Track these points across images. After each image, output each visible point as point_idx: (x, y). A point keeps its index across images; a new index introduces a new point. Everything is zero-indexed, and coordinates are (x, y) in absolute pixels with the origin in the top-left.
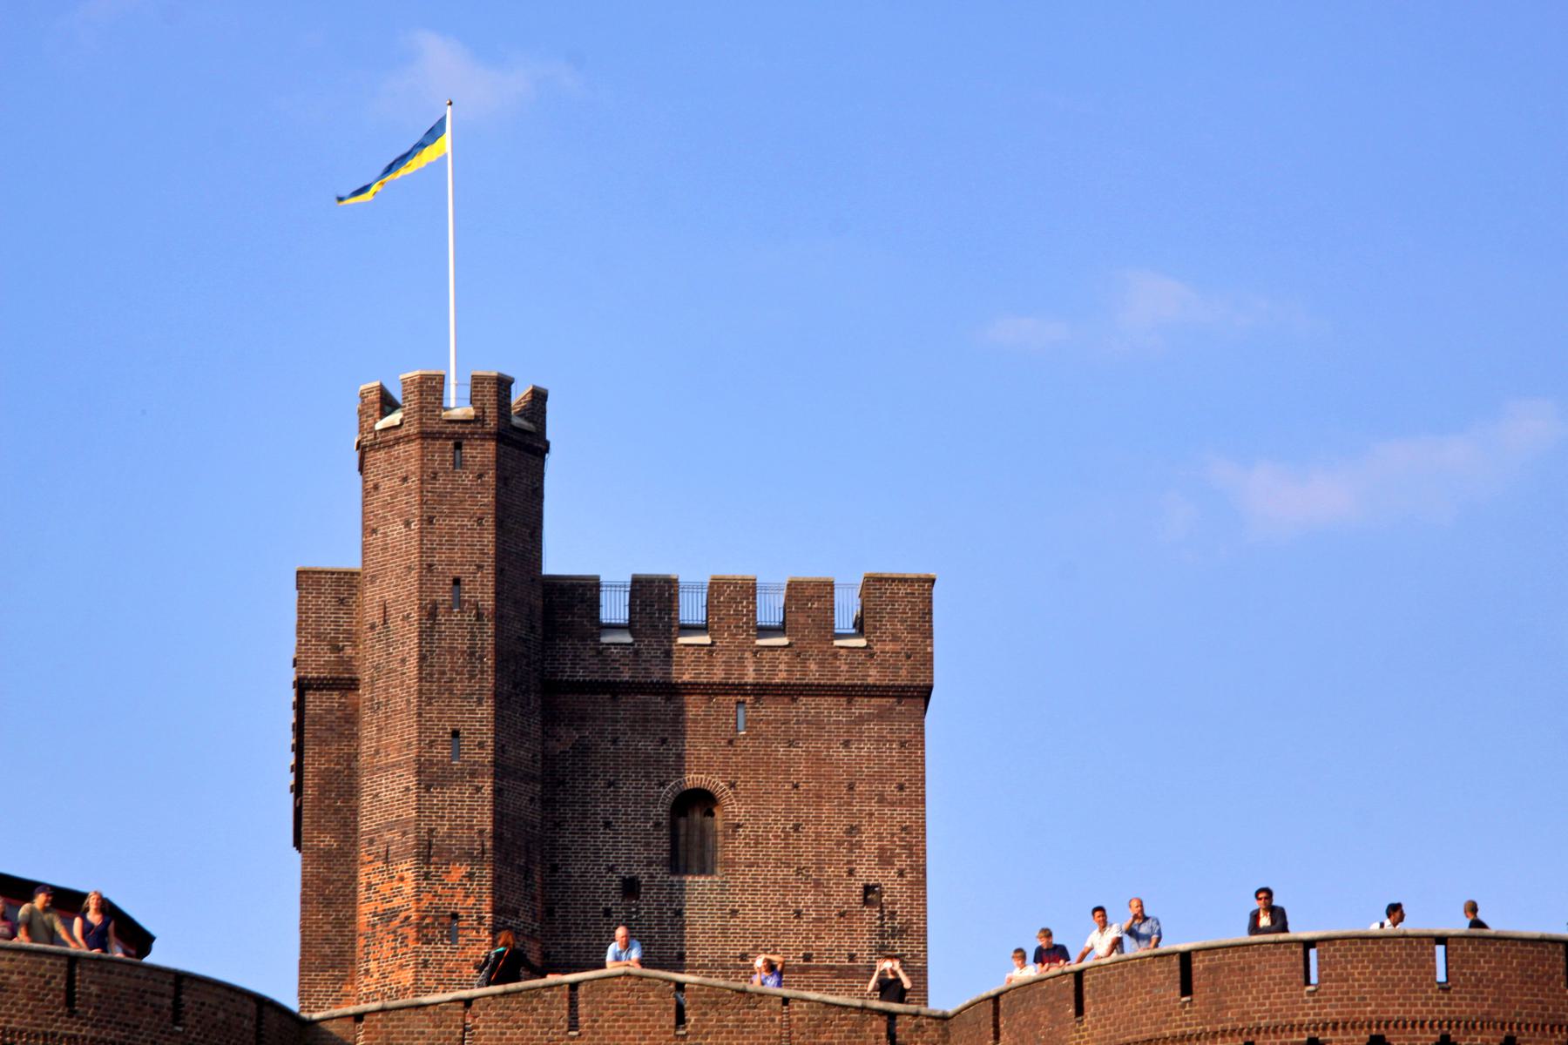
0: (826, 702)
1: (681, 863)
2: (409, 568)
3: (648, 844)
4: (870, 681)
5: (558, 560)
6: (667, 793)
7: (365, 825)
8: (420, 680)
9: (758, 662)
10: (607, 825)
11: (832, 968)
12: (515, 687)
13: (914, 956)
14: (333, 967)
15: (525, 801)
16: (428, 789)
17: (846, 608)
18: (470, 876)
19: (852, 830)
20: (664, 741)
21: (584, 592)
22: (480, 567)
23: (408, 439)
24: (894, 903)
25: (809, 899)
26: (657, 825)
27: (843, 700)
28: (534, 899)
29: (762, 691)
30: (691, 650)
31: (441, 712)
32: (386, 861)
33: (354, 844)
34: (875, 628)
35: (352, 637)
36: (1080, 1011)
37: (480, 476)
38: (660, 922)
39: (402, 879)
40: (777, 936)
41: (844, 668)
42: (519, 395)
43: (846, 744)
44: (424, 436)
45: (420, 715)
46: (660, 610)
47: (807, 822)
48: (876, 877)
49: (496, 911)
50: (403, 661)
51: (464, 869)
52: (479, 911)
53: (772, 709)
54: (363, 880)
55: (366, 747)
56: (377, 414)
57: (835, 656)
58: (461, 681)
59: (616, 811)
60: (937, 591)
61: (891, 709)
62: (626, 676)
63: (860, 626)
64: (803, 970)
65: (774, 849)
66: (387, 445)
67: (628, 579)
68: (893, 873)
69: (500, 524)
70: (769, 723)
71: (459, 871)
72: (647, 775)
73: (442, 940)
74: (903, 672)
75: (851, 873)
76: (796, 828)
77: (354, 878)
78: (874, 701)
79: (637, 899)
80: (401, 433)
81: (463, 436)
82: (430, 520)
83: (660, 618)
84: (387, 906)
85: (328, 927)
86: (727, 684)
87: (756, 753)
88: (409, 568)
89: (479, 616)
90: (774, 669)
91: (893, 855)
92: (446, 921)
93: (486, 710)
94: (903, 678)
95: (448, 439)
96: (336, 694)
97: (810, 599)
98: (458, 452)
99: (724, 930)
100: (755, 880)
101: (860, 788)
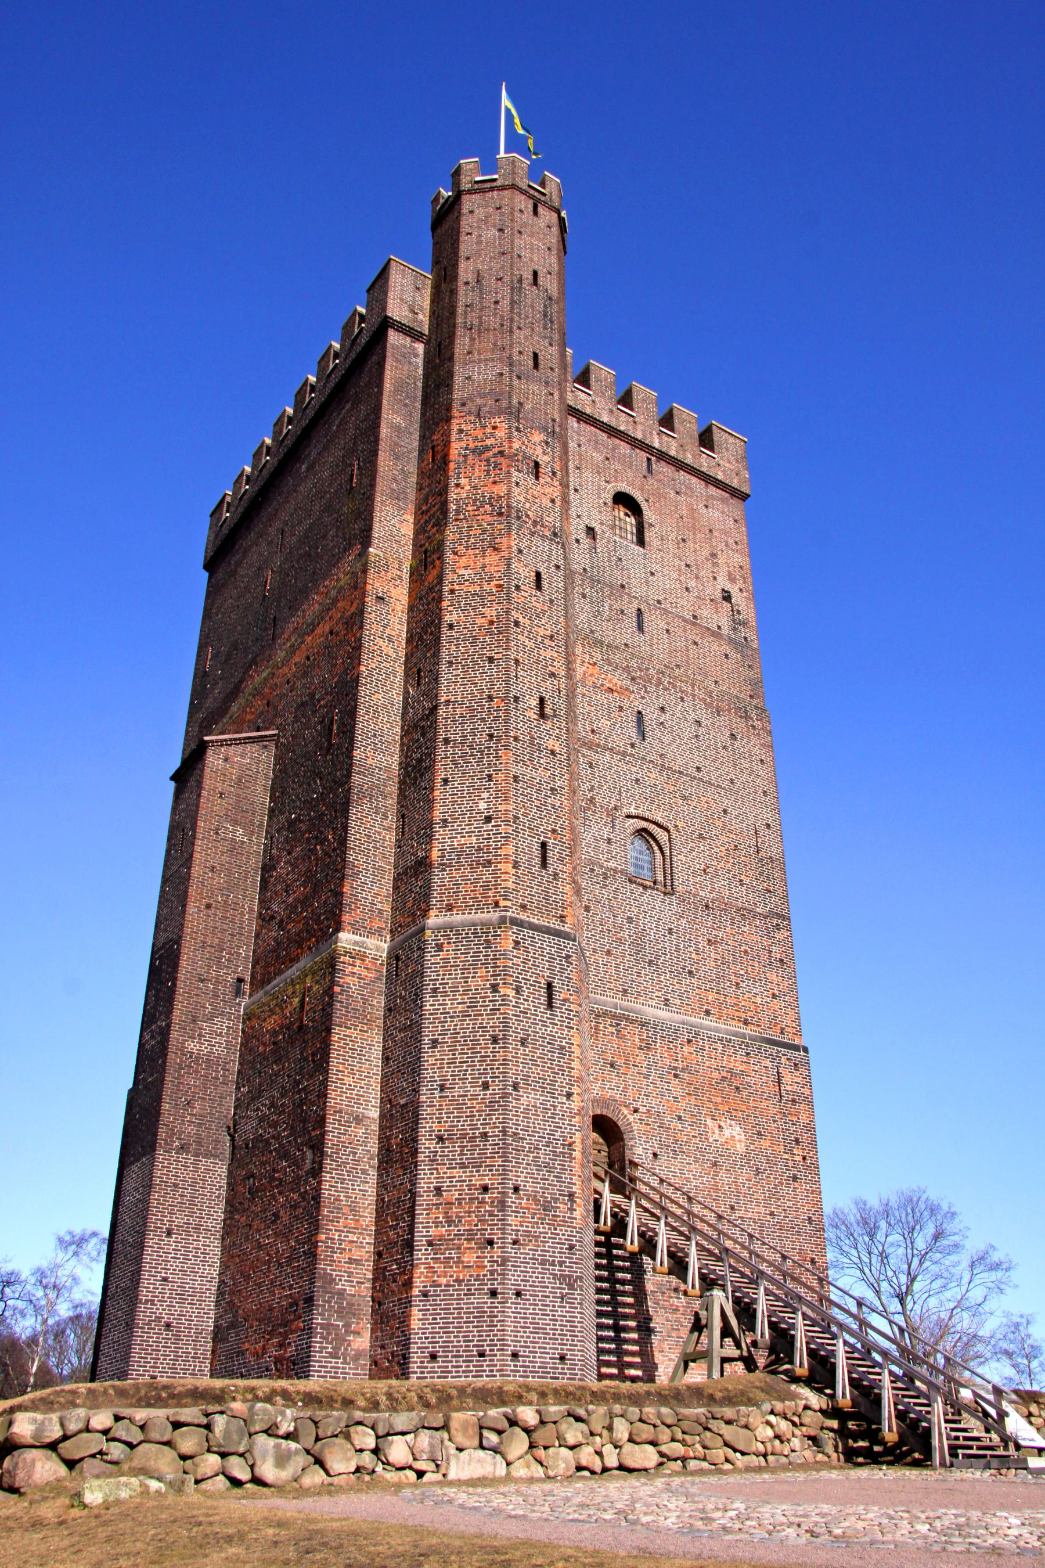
0: (694, 480)
6: (611, 489)
11: (709, 629)
19: (714, 555)
23: (503, 188)
29: (663, 456)
32: (479, 416)
38: (609, 561)
48: (728, 587)
65: (671, 546)
66: (483, 191)
72: (598, 473)
75: (715, 578)
78: (718, 491)
80: (495, 184)
84: (483, 443)
90: (669, 447)
92: (532, 464)
96: (408, 339)
99: (647, 582)
100: (662, 557)
101: (715, 534)
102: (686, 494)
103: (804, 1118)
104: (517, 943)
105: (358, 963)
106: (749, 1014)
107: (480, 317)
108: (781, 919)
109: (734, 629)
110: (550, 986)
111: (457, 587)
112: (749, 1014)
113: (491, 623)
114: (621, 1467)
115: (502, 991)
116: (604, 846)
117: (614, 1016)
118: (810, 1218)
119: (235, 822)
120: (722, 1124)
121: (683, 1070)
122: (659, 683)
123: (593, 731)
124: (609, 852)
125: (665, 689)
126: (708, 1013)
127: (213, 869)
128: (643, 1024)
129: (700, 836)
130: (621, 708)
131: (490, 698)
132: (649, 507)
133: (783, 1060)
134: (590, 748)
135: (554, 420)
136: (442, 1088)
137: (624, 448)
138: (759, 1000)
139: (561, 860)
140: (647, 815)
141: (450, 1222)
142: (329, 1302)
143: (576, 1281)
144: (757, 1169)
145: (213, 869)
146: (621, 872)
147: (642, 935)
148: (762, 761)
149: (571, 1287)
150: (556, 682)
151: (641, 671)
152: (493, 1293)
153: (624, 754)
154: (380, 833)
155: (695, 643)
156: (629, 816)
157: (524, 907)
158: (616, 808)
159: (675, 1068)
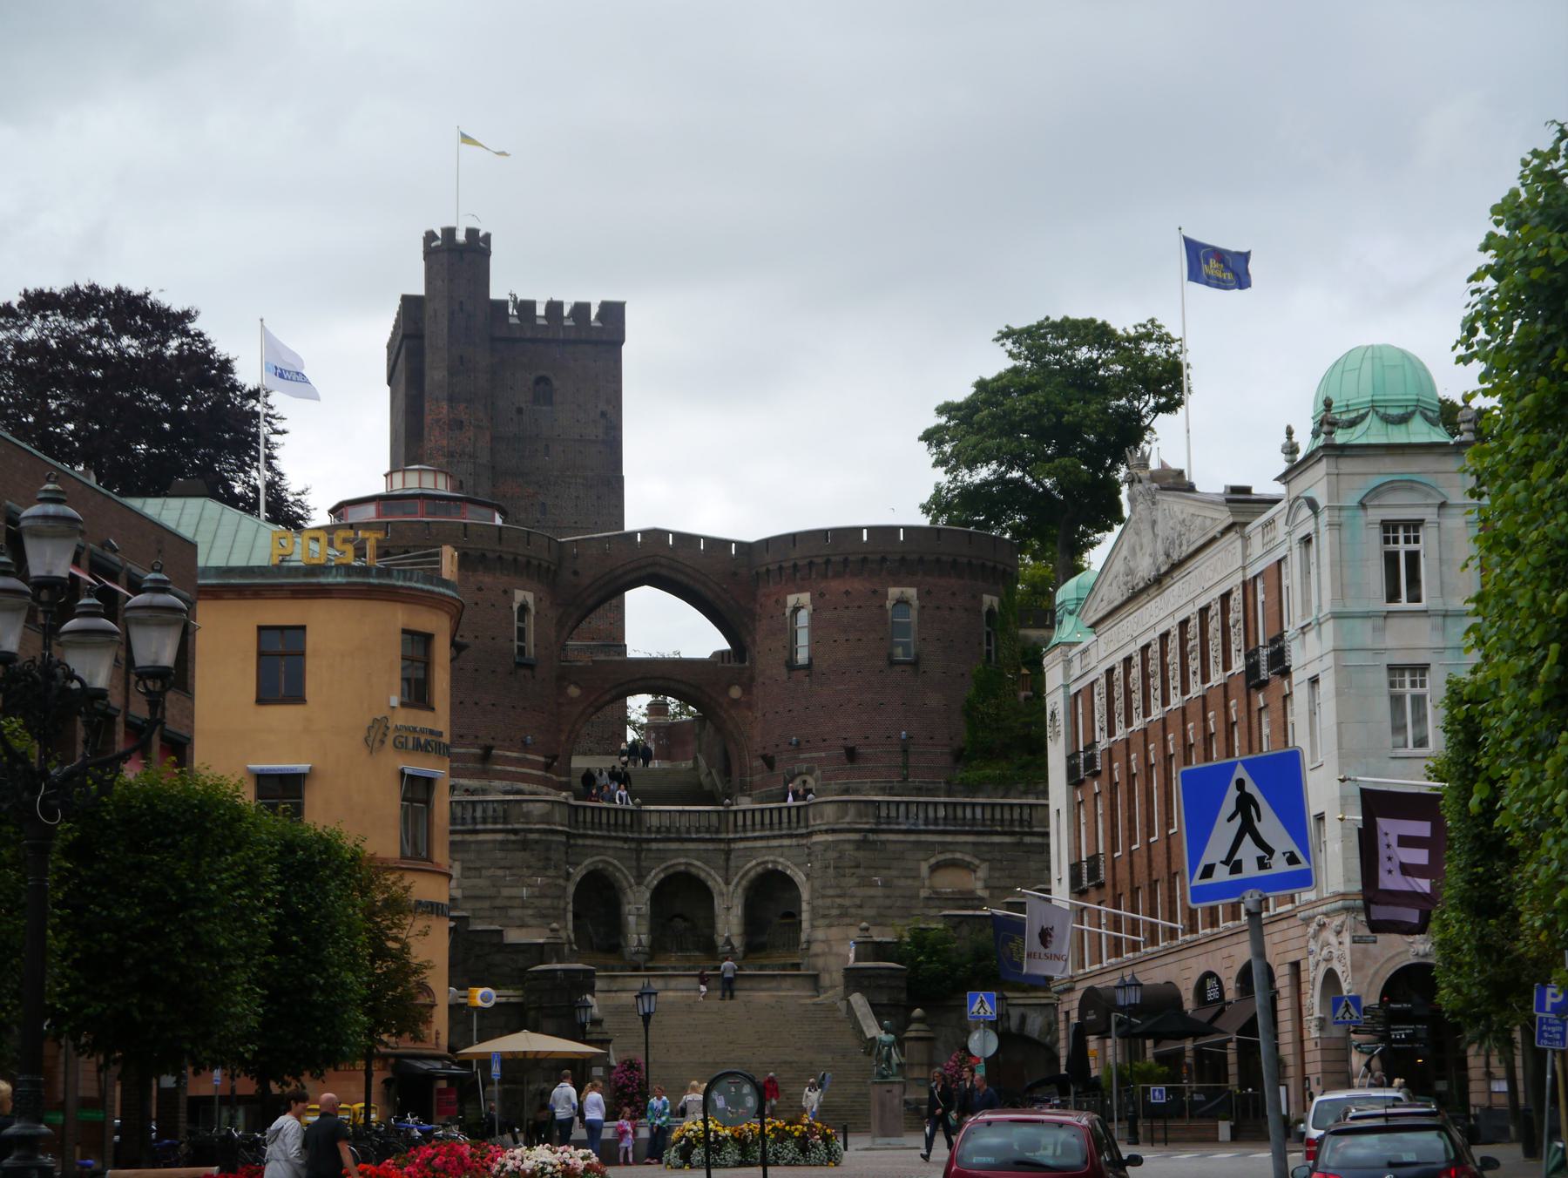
7: (427, 388)
36: (795, 545)
42: (481, 234)
43: (595, 361)
68: (611, 407)
71: (463, 406)
75: (596, 407)
155: (580, 452)
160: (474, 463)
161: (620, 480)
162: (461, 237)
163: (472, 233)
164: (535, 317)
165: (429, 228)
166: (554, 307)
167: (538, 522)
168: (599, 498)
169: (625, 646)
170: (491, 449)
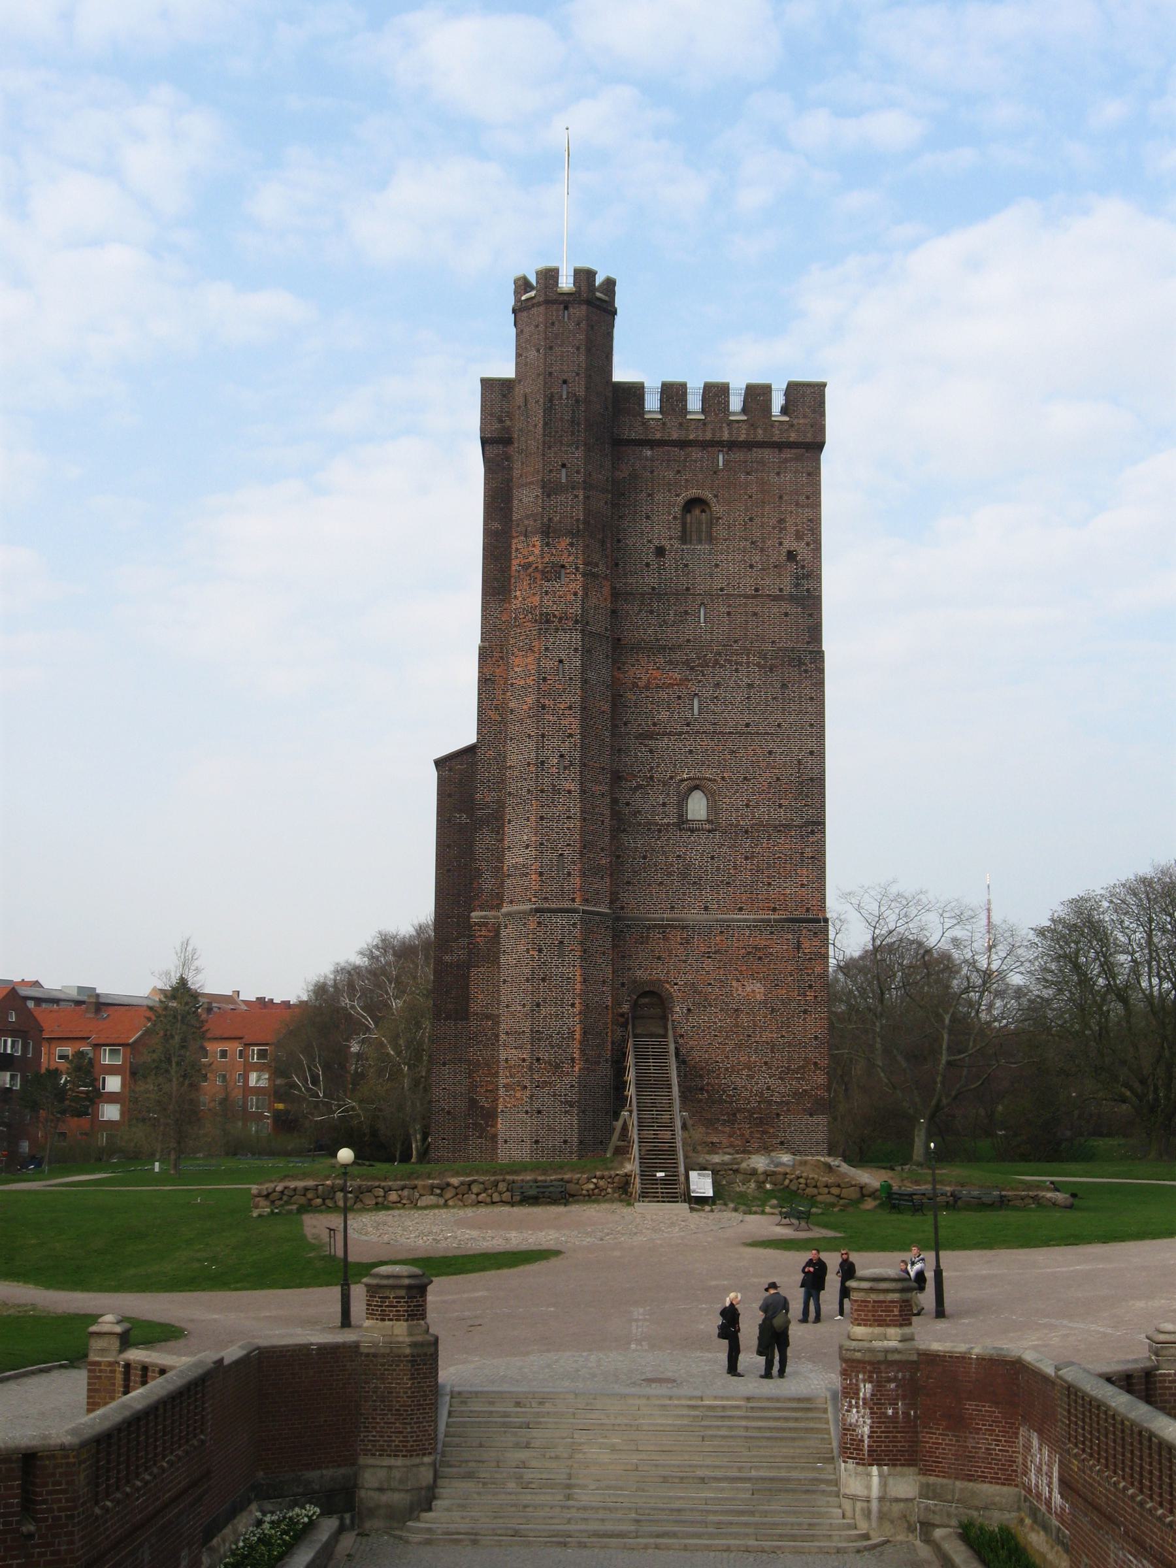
0: (767, 454)
1: (688, 538)
2: (539, 375)
3: (670, 528)
4: (791, 439)
5: (621, 373)
6: (681, 500)
7: (515, 517)
8: (544, 436)
9: (730, 430)
10: (648, 517)
11: (770, 595)
12: (597, 441)
13: (815, 589)
14: (499, 594)
15: (602, 503)
16: (549, 496)
17: (778, 401)
18: (571, 545)
19: (781, 521)
20: (679, 472)
21: (635, 392)
22: (578, 374)
23: (539, 304)
24: (804, 560)
25: (757, 558)
26: (675, 518)
27: (776, 450)
28: (607, 557)
29: (732, 445)
30: (693, 422)
31: (555, 453)
32: (526, 536)
33: (511, 528)
34: (794, 410)
35: (510, 415)
37: (578, 324)
39: (534, 546)
40: (740, 578)
41: (777, 432)
42: (599, 280)
43: (778, 474)
44: (548, 302)
45: (544, 455)
46: (677, 401)
47: (757, 516)
49: (586, 564)
50: (536, 425)
51: (568, 540)
52: (576, 564)
53: (738, 455)
54: (514, 547)
55: (516, 473)
56: (522, 292)
57: (772, 426)
58: (567, 436)
59: (652, 510)
60: (829, 392)
61: (803, 455)
62: (658, 436)
63: (785, 410)
64: (754, 597)
67: (660, 385)
69: (588, 350)
70: (735, 462)
72: (669, 491)
73: (555, 580)
74: (809, 435)
75: (781, 544)
76: (751, 519)
77: (510, 546)
78: (793, 451)
79: (664, 557)
80: (534, 301)
81: (569, 302)
82: (551, 348)
83: (677, 405)
84: (527, 561)
85: (495, 572)
86: (713, 441)
87: (729, 478)
88: (539, 375)
89: (577, 401)
91: (804, 534)
93: (579, 453)
94: (809, 438)
95: (560, 304)
96: (501, 447)
97: (759, 395)
98: (566, 312)
99: (711, 576)
101: (785, 498)
102: (757, 471)
103: (818, 970)
104: (539, 923)
105: (484, 928)
106: (778, 903)
107: (526, 442)
108: (817, 825)
109: (797, 585)
110: (561, 942)
111: (514, 681)
112: (778, 903)
113: (530, 709)
114: (502, 1202)
115: (531, 953)
116: (660, 809)
117: (662, 926)
118: (816, 1038)
119: (460, 811)
120: (746, 983)
121: (715, 953)
122: (716, 662)
123: (655, 724)
124: (664, 812)
125: (722, 666)
126: (741, 909)
127: (449, 846)
128: (683, 928)
129: (745, 778)
130: (679, 698)
131: (529, 764)
132: (718, 501)
133: (804, 932)
134: (651, 738)
135: (578, 520)
136: (507, 1006)
137: (696, 453)
138: (788, 891)
139: (574, 863)
140: (698, 774)
141: (511, 1076)
142: (476, 1112)
143: (574, 1103)
144: (773, 1009)
145: (449, 846)
146: (673, 824)
147: (687, 867)
148: (812, 698)
149: (571, 1106)
150: (572, 740)
151: (699, 659)
152: (527, 1112)
153: (681, 734)
154: (494, 845)
155: (755, 614)
156: (683, 780)
157: (545, 898)
158: (671, 778)
159: (709, 952)
160: (582, 631)
161: (818, 657)
162: (566, 283)
163: (584, 276)
164: (684, 410)
165: (520, 274)
166: (716, 394)
167: (688, 725)
168: (784, 686)
169: (826, 920)
170: (614, 612)
